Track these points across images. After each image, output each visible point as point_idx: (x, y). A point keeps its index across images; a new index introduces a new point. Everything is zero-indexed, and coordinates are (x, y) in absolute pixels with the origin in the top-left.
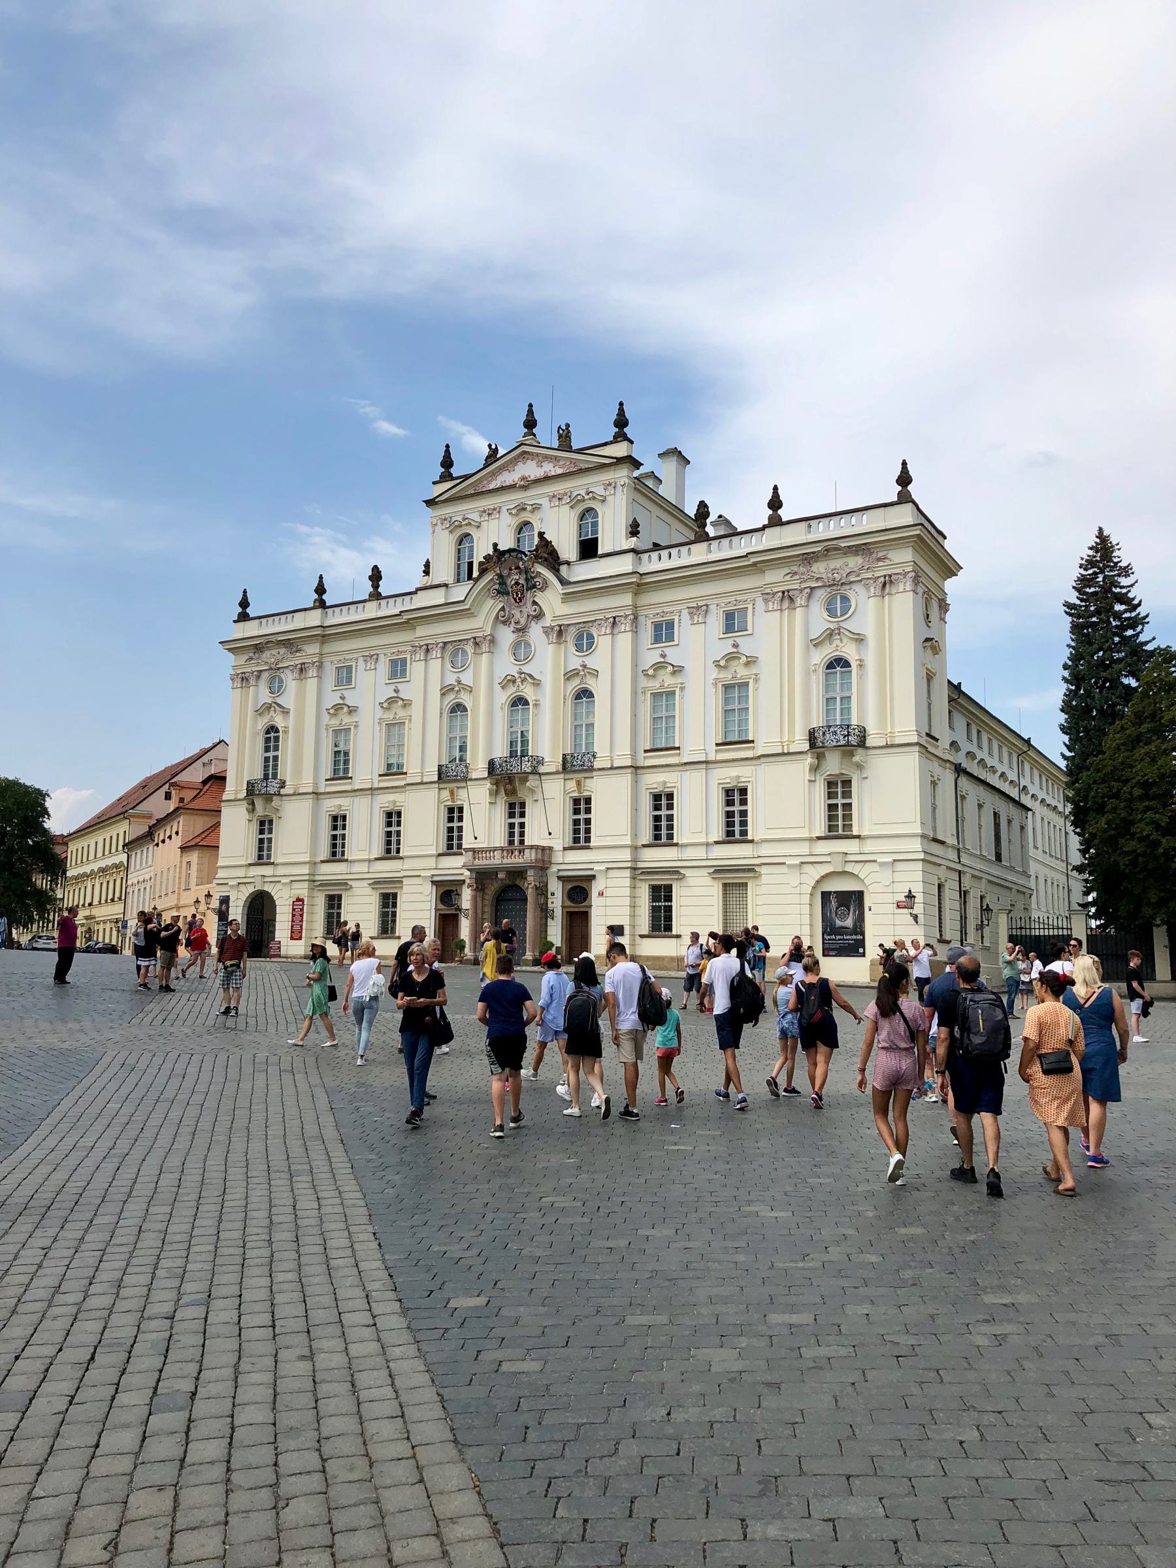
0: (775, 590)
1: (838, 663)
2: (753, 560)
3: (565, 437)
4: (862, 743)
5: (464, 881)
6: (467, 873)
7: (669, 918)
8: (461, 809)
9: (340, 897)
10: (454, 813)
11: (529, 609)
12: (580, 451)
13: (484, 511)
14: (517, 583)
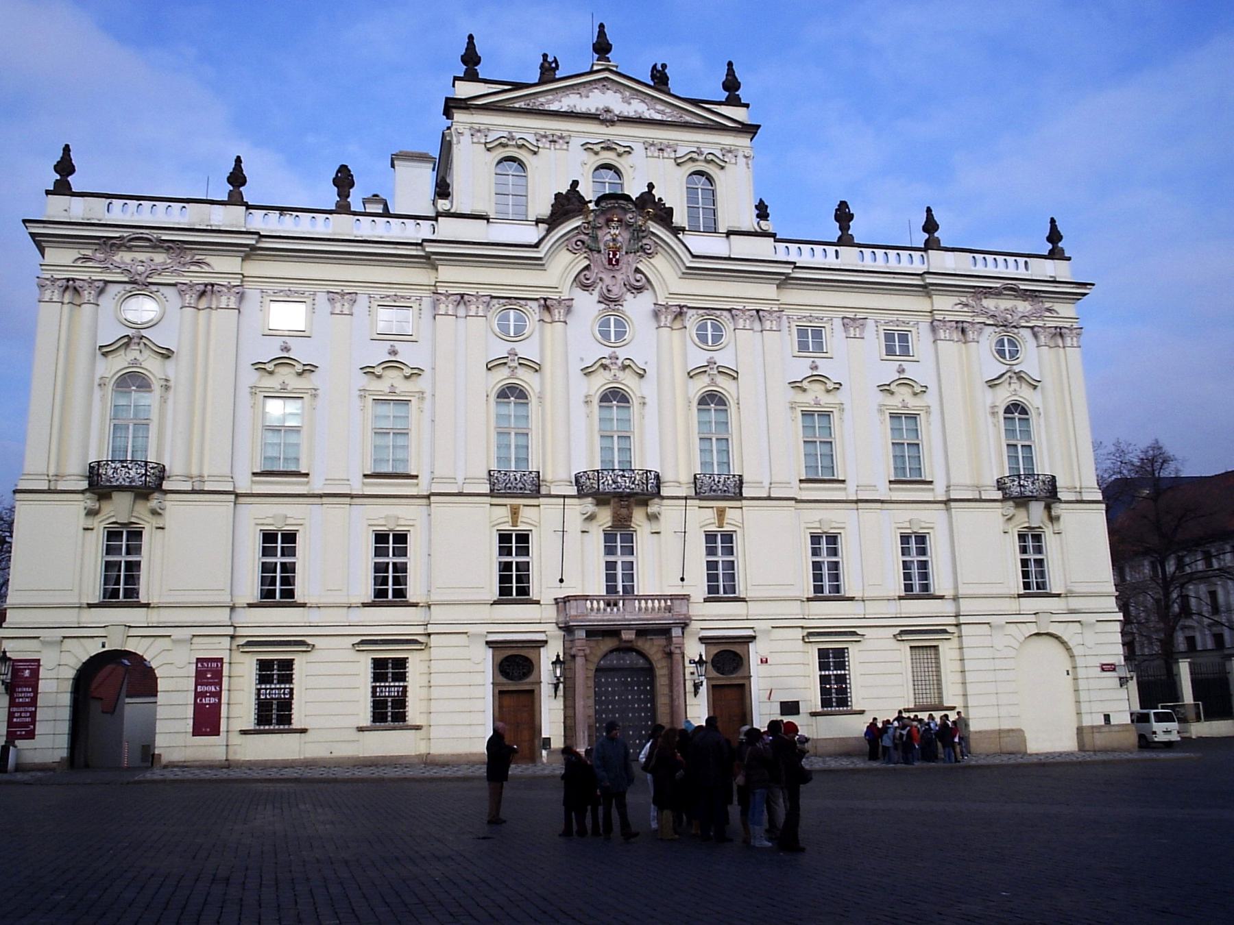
1: (1016, 409)
2: (928, 281)
3: (660, 78)
6: (552, 629)
8: (523, 538)
10: (514, 543)
13: (545, 136)
14: (614, 240)
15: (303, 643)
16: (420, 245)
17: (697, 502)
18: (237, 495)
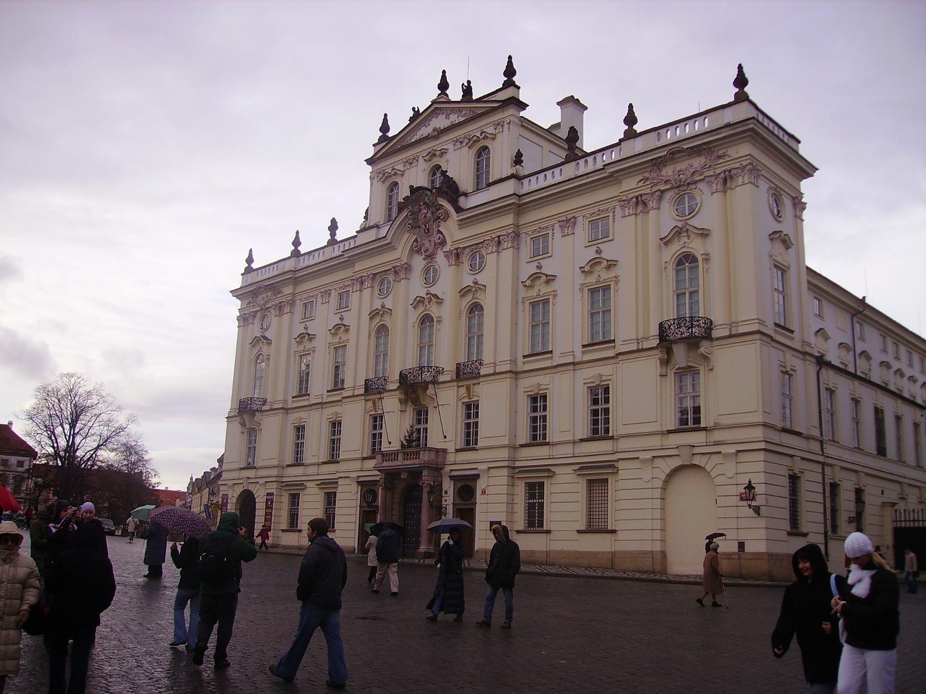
0: (630, 196)
1: (686, 260)
3: (467, 90)
4: (708, 336)
7: (541, 515)
11: (436, 238)
12: (479, 100)
13: (407, 162)
17: (455, 383)
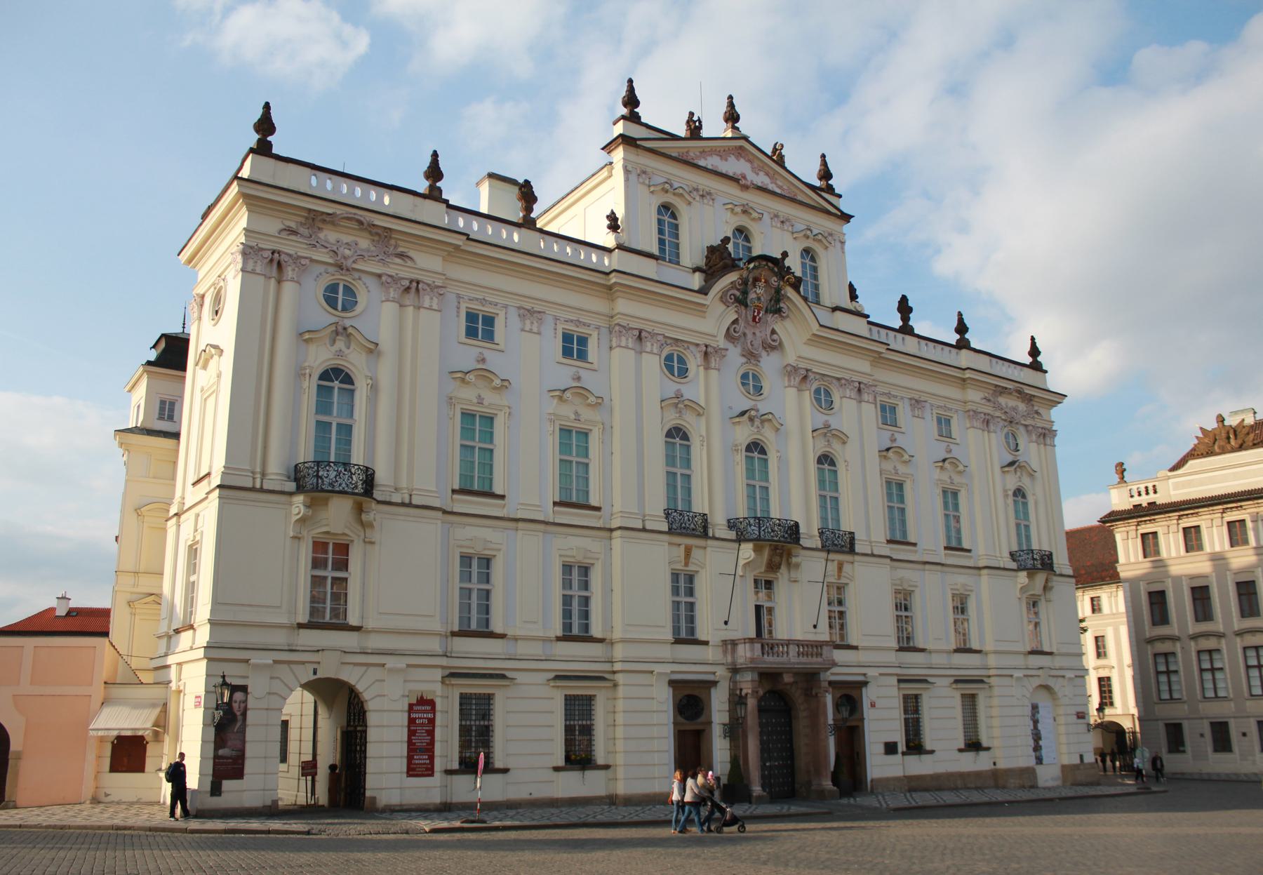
3: (777, 157)
5: (714, 683)
6: (721, 673)
8: (690, 578)
9: (489, 698)
10: (683, 583)
11: (762, 333)
13: (697, 190)
15: (503, 677)
16: (607, 274)
18: (445, 512)
